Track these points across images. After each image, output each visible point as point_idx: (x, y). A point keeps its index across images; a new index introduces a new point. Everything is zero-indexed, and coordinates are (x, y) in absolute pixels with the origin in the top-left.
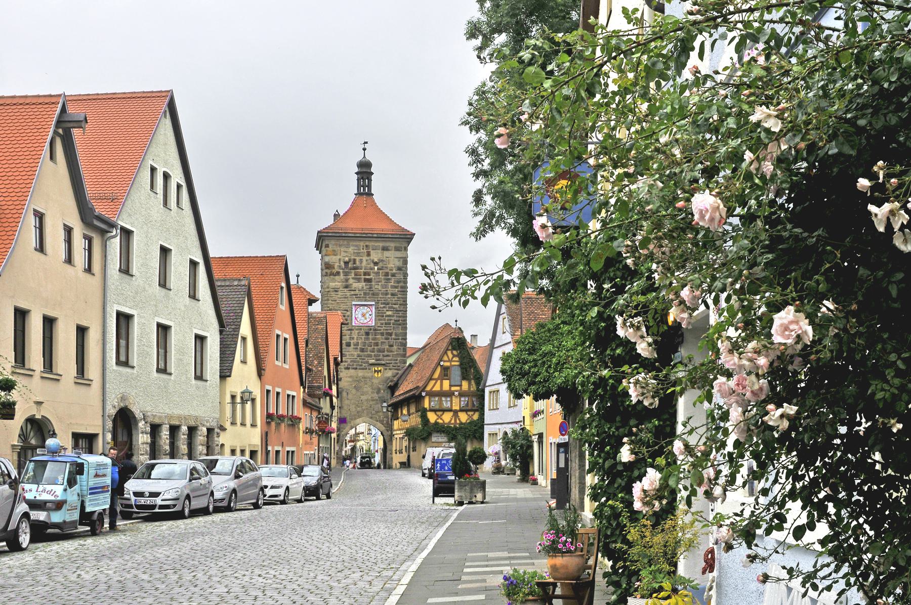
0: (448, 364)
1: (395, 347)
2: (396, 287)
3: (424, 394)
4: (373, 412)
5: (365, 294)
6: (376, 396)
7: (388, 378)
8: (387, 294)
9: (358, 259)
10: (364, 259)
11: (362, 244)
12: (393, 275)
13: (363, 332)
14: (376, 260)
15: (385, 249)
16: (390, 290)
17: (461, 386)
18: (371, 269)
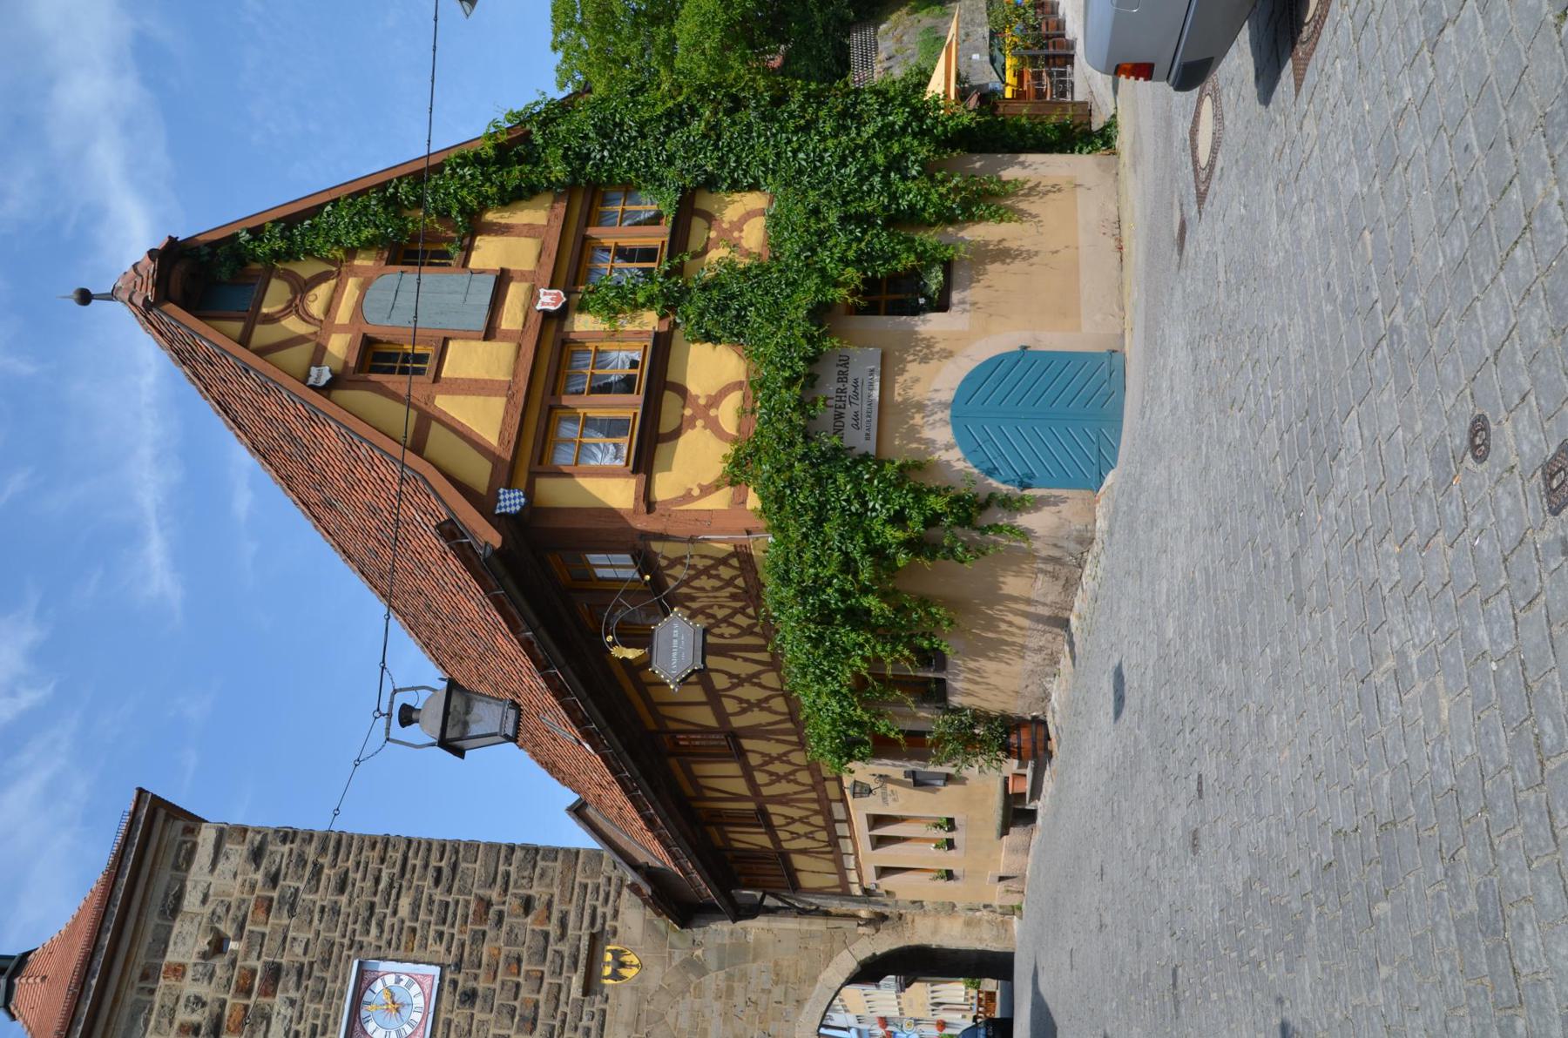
0: (339, 346)
1: (537, 891)
2: (318, 870)
3: (511, 501)
4: (778, 993)
5: (318, 995)
6: (714, 980)
7: (648, 923)
8: (336, 911)
9: (183, 1016)
10: (189, 988)
11: (131, 996)
12: (273, 880)
13: (459, 1017)
14: (204, 944)
15: (173, 909)
16: (324, 896)
17: (503, 279)
18: (233, 963)
